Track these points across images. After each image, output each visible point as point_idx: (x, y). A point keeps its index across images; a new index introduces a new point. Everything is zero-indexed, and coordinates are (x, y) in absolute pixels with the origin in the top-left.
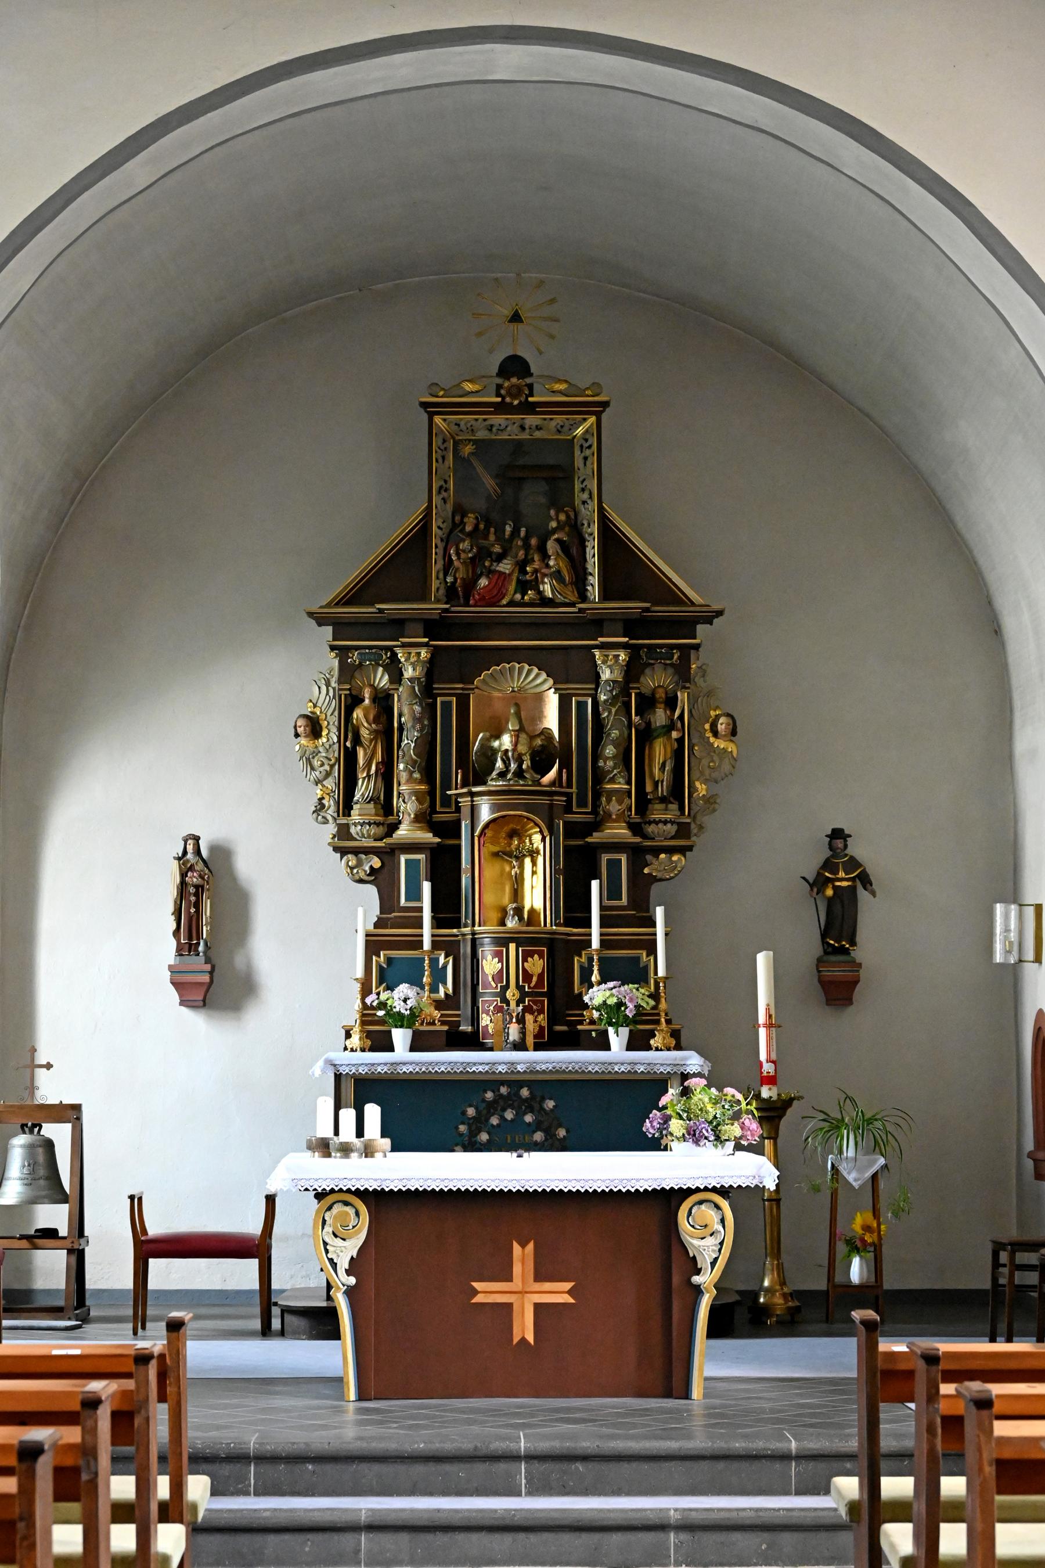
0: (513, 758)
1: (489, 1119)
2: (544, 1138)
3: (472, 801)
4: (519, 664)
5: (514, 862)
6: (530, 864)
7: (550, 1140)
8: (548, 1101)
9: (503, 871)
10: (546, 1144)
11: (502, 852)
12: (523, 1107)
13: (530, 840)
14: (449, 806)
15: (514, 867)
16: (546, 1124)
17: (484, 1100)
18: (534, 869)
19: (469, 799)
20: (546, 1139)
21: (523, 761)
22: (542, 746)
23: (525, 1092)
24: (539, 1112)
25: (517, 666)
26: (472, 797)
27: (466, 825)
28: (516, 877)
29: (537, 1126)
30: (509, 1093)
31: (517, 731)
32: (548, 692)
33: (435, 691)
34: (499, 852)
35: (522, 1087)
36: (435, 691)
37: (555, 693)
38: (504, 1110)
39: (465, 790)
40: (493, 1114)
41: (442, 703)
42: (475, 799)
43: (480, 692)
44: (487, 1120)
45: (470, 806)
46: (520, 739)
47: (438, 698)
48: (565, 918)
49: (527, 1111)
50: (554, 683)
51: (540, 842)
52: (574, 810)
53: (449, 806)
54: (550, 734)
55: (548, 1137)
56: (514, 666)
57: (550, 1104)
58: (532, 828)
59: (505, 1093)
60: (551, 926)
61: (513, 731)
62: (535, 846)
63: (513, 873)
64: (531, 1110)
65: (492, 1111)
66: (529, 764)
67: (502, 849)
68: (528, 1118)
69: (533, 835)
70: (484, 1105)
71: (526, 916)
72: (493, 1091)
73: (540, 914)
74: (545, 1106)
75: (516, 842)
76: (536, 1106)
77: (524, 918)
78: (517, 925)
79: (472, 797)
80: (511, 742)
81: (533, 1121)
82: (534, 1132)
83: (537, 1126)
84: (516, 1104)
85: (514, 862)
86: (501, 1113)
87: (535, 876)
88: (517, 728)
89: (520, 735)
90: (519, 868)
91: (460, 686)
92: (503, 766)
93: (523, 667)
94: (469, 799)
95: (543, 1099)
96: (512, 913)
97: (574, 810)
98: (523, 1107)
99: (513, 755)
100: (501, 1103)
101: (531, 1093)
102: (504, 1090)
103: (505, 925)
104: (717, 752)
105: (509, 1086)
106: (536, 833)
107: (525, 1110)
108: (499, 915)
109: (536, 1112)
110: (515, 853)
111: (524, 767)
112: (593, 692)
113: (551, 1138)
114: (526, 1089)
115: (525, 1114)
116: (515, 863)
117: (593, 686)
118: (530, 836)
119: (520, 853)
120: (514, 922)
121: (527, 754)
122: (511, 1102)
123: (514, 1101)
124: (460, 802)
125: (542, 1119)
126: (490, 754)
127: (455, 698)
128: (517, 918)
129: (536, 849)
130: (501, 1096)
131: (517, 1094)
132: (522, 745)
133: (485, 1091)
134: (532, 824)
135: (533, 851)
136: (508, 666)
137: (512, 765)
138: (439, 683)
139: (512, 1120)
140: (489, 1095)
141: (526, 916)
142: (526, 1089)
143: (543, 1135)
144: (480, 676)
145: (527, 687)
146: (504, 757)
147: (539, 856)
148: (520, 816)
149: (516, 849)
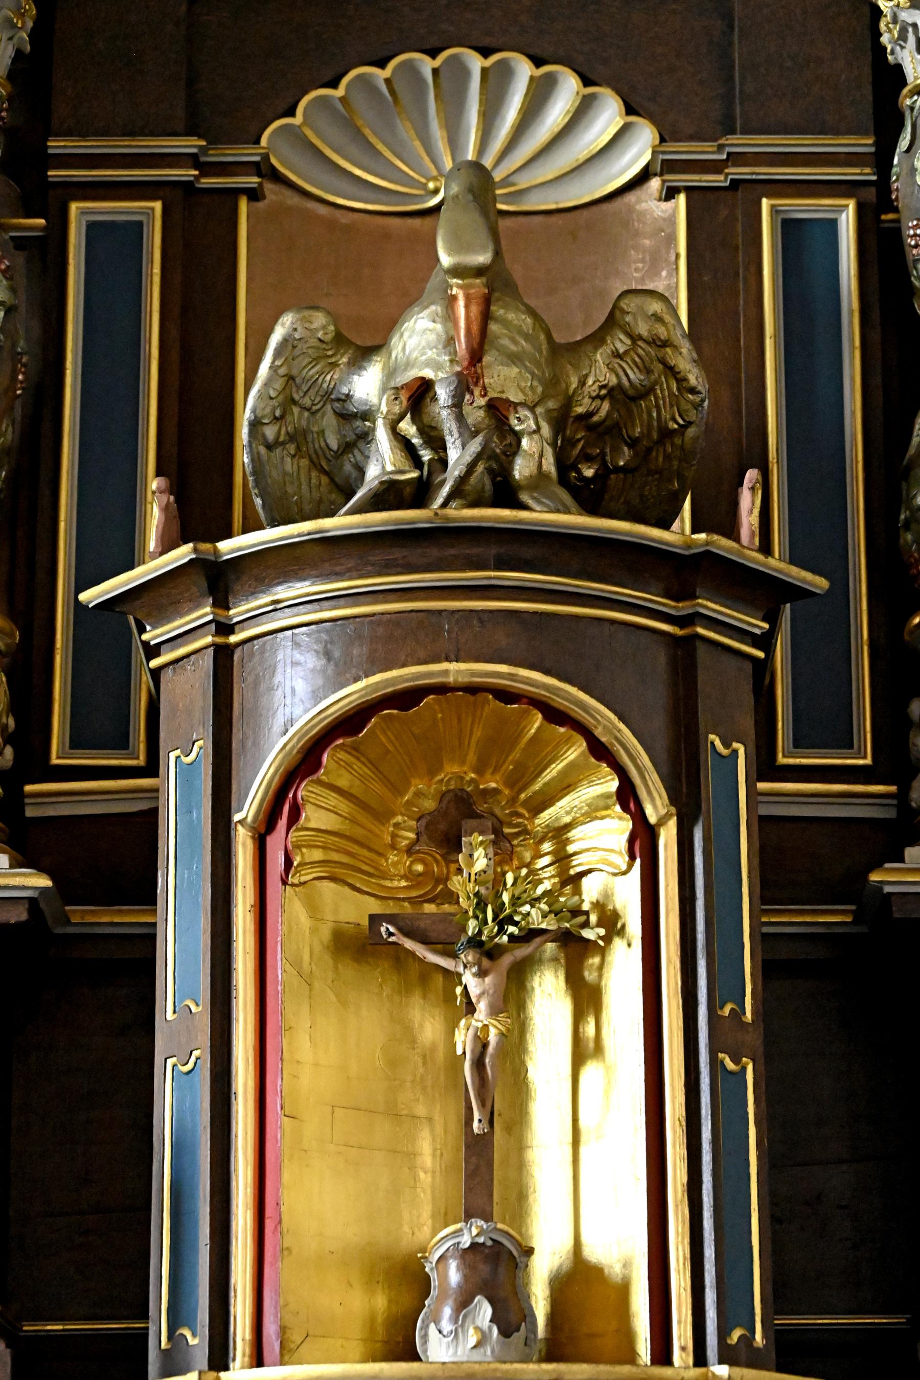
0: (460, 418)
3: (225, 628)
4: (486, 52)
5: (469, 978)
6: (564, 1006)
9: (409, 1035)
11: (390, 919)
13: (562, 859)
14: (121, 742)
15: (470, 1008)
18: (589, 1029)
19: (205, 613)
21: (518, 436)
22: (613, 393)
25: (476, 63)
26: (222, 603)
27: (186, 773)
28: (479, 1064)
31: (479, 271)
32: (631, 197)
33: (53, 174)
34: (375, 920)
36: (53, 174)
37: (670, 194)
39: (183, 554)
41: (95, 230)
42: (237, 612)
43: (294, 200)
45: (207, 661)
46: (493, 327)
47: (74, 207)
48: (776, 1335)
50: (663, 140)
51: (622, 861)
52: (782, 760)
53: (121, 742)
54: (657, 318)
56: (461, 71)
58: (565, 786)
60: (700, 1359)
61: (457, 271)
62: (591, 889)
63: (463, 1039)
66: (549, 464)
67: (391, 908)
69: (568, 827)
71: (540, 1307)
73: (624, 1290)
75: (481, 862)
77: (528, 1315)
78: (488, 1351)
79: (222, 603)
80: (450, 341)
85: (469, 978)
87: (590, 1071)
88: (483, 258)
89: (498, 310)
90: (494, 1012)
91: (189, 145)
92: (405, 464)
93: (505, 73)
94: (205, 613)
96: (454, 1275)
97: (782, 760)
99: (457, 405)
103: (413, 1355)
106: (593, 812)
108: (381, 1302)
110: (472, 926)
111: (521, 469)
112: (867, 174)
116: (474, 992)
117: (865, 144)
118: (560, 833)
119: (502, 924)
120: (472, 1340)
121: (539, 410)
124: (152, 651)
126: (334, 444)
127: (158, 206)
128: (484, 1311)
129: (599, 906)
132: (514, 359)
134: (576, 751)
135: (576, 912)
136: (427, 65)
137: (453, 454)
138: (68, 133)
141: (540, 1307)
144: (291, 113)
145: (523, 181)
146: (408, 427)
147: (618, 944)
148: (505, 696)
149: (481, 905)
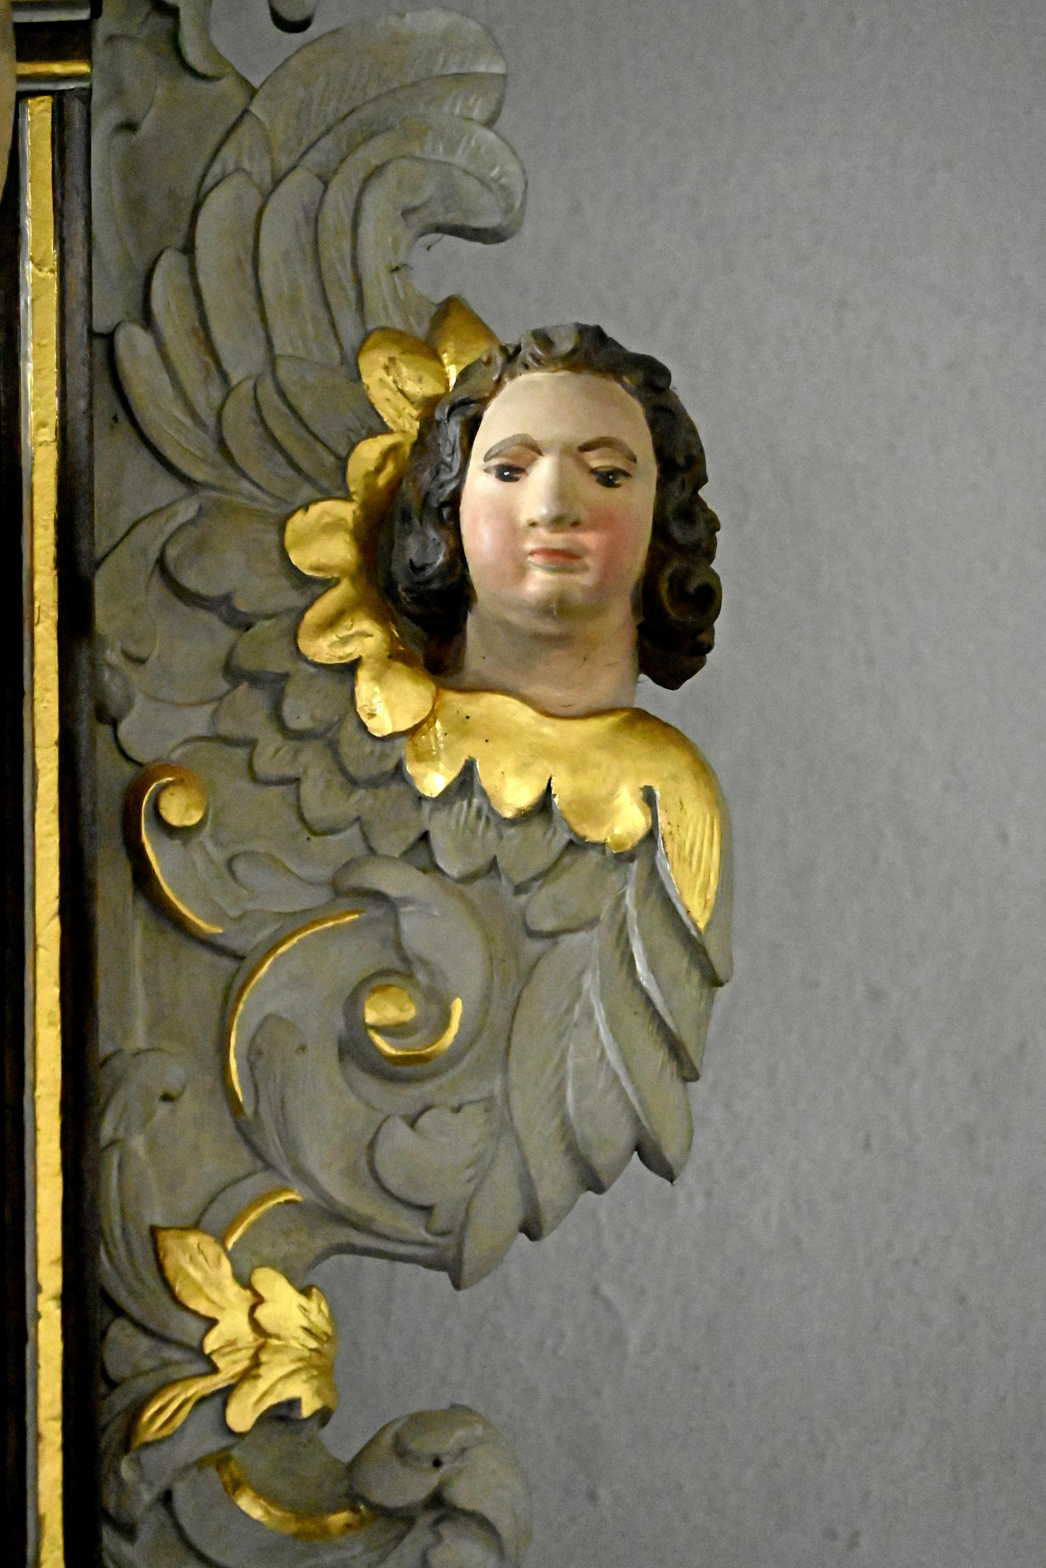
104: (452, 865)
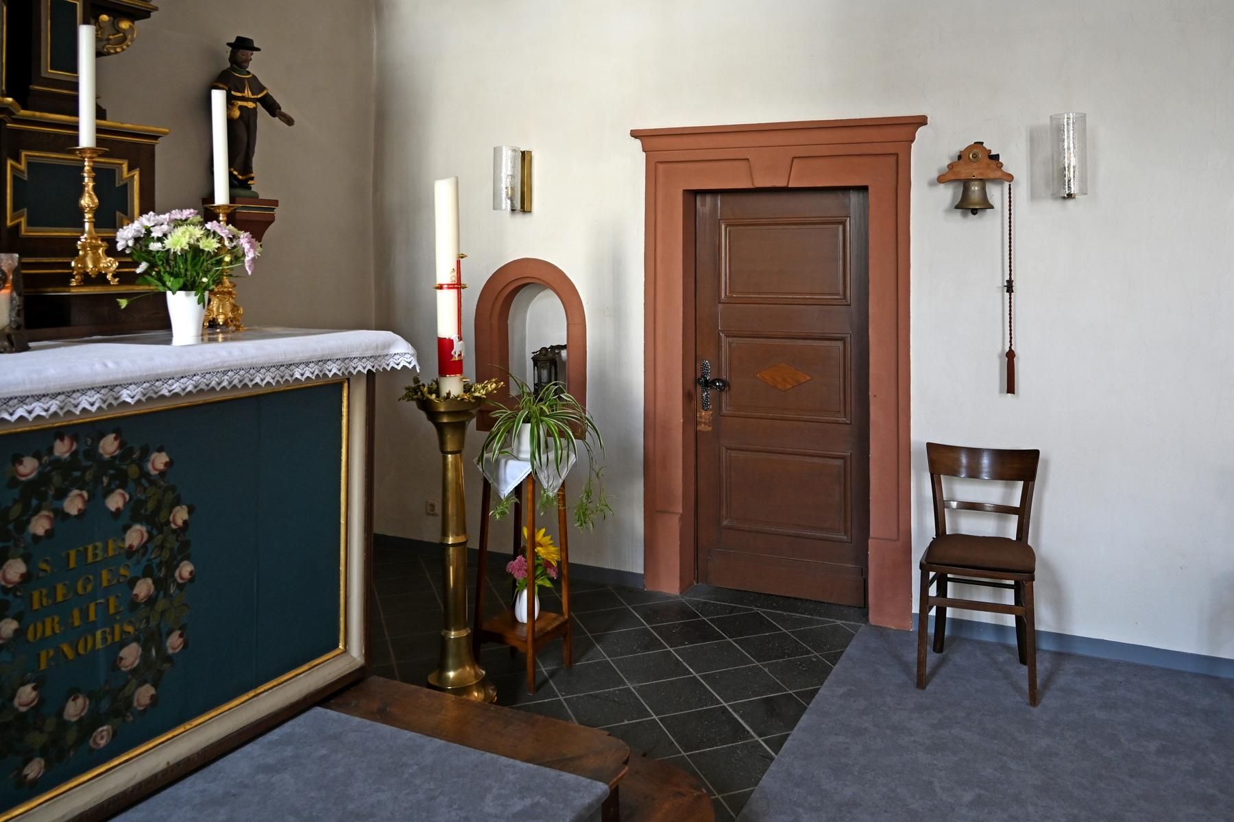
1: (28, 522)
2: (146, 536)
7: (160, 537)
8: (155, 455)
10: (150, 546)
12: (105, 480)
16: (151, 505)
17: (14, 482)
20: (151, 537)
23: (109, 446)
24: (137, 482)
29: (135, 512)
30: (74, 454)
35: (103, 435)
38: (62, 494)
40: (36, 511)
44: (23, 525)
49: (113, 486)
55: (155, 532)
57: (159, 461)
59: (67, 455)
64: (121, 480)
65: (34, 502)
68: (115, 501)
70: (16, 493)
72: (37, 456)
74: (150, 467)
76: (133, 471)
81: (125, 504)
82: (126, 528)
83: (135, 512)
84: (89, 476)
86: (56, 504)
95: (145, 453)
98: (105, 480)
100: (57, 479)
101: (121, 446)
102: (62, 449)
105: (75, 438)
107: (109, 484)
109: (131, 485)
113: (161, 531)
114: (112, 436)
115: (108, 492)
122: (77, 474)
123: (84, 470)
125: (143, 497)
130: (57, 464)
131: (92, 453)
133: (18, 460)
139: (82, 513)
140: (28, 467)
142: (112, 436)
143: (144, 529)
